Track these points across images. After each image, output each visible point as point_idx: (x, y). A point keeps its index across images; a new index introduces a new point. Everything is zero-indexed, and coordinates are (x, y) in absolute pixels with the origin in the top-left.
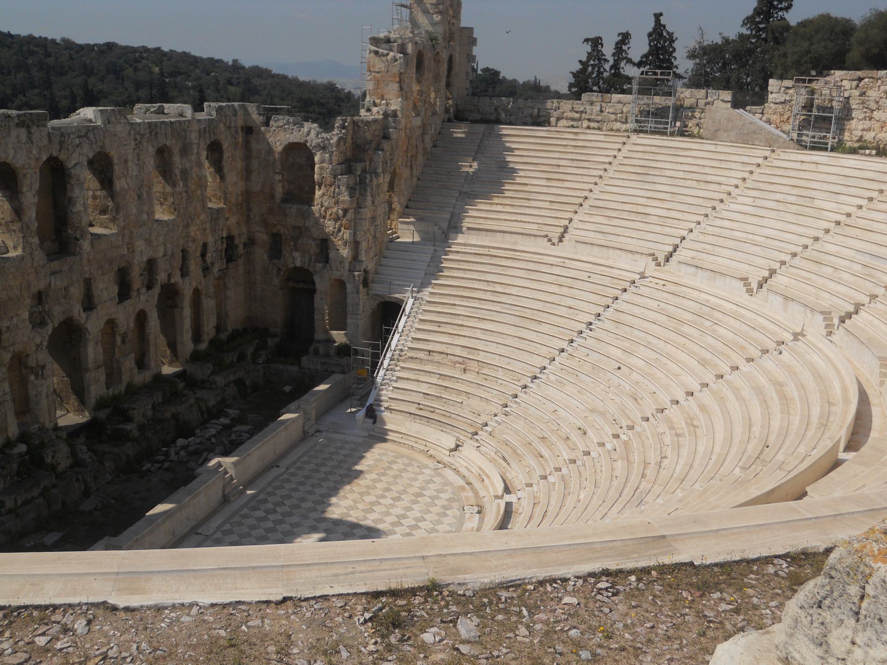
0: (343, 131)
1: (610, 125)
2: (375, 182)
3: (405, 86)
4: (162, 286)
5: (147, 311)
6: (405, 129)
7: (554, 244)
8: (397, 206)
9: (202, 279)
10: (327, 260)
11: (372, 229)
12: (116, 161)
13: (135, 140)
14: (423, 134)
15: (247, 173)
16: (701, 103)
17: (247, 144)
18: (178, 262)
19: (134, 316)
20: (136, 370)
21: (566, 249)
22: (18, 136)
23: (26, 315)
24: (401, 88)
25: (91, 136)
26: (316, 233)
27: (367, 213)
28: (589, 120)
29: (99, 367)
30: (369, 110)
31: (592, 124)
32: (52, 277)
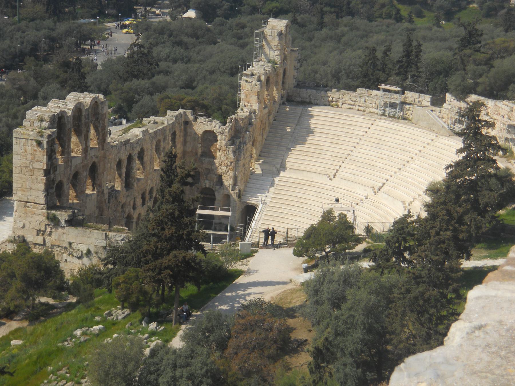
0: (231, 124)
1: (370, 110)
2: (245, 148)
3: (260, 97)
7: (331, 179)
8: (255, 156)
11: (243, 170)
12: (145, 150)
14: (269, 116)
15: (185, 142)
16: (417, 100)
21: (335, 182)
24: (258, 98)
27: (241, 163)
28: (359, 106)
30: (242, 110)
31: (361, 108)
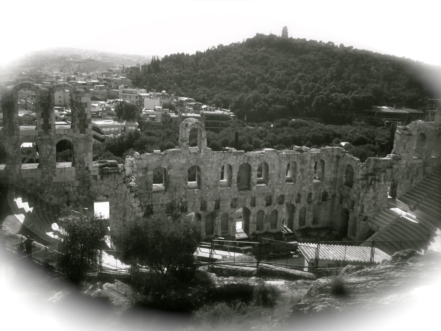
3: (406, 148)
6: (406, 164)
9: (307, 205)
10: (353, 209)
12: (269, 165)
13: (279, 159)
17: (337, 162)
18: (296, 197)
20: (270, 227)
23: (229, 204)
24: (405, 149)
25: (261, 158)
26: (351, 199)
29: (254, 223)
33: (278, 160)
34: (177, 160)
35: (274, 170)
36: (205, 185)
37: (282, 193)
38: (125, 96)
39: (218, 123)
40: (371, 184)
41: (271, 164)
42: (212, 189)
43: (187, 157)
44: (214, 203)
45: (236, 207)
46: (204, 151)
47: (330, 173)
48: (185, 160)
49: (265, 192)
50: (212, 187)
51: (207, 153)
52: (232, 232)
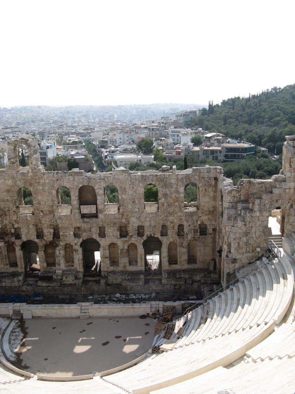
3: (292, 165)
4: (148, 237)
5: (137, 245)
9: (177, 239)
13: (131, 181)
19: (127, 245)
20: (128, 264)
22: (69, 178)
23: (72, 233)
25: (106, 179)
29: (106, 258)
32: (83, 224)
33: (130, 182)
34: (3, 181)
35: (125, 194)
36: (38, 209)
37: (140, 224)
38: (174, 136)
39: (239, 155)
40: (240, 215)
41: (121, 187)
42: (46, 215)
43: (13, 178)
44: (52, 231)
45: (80, 237)
46: (32, 171)
47: (208, 200)
48: (11, 181)
49: (116, 221)
50: (48, 213)
51: (35, 172)
52: (78, 266)
